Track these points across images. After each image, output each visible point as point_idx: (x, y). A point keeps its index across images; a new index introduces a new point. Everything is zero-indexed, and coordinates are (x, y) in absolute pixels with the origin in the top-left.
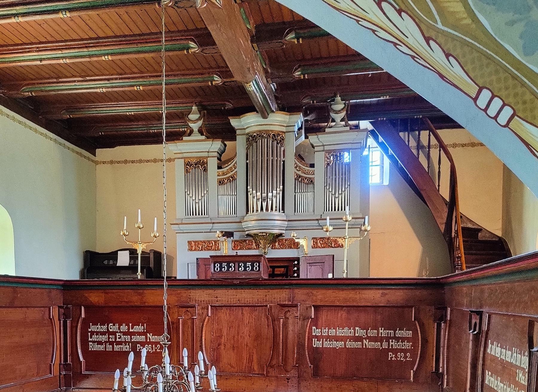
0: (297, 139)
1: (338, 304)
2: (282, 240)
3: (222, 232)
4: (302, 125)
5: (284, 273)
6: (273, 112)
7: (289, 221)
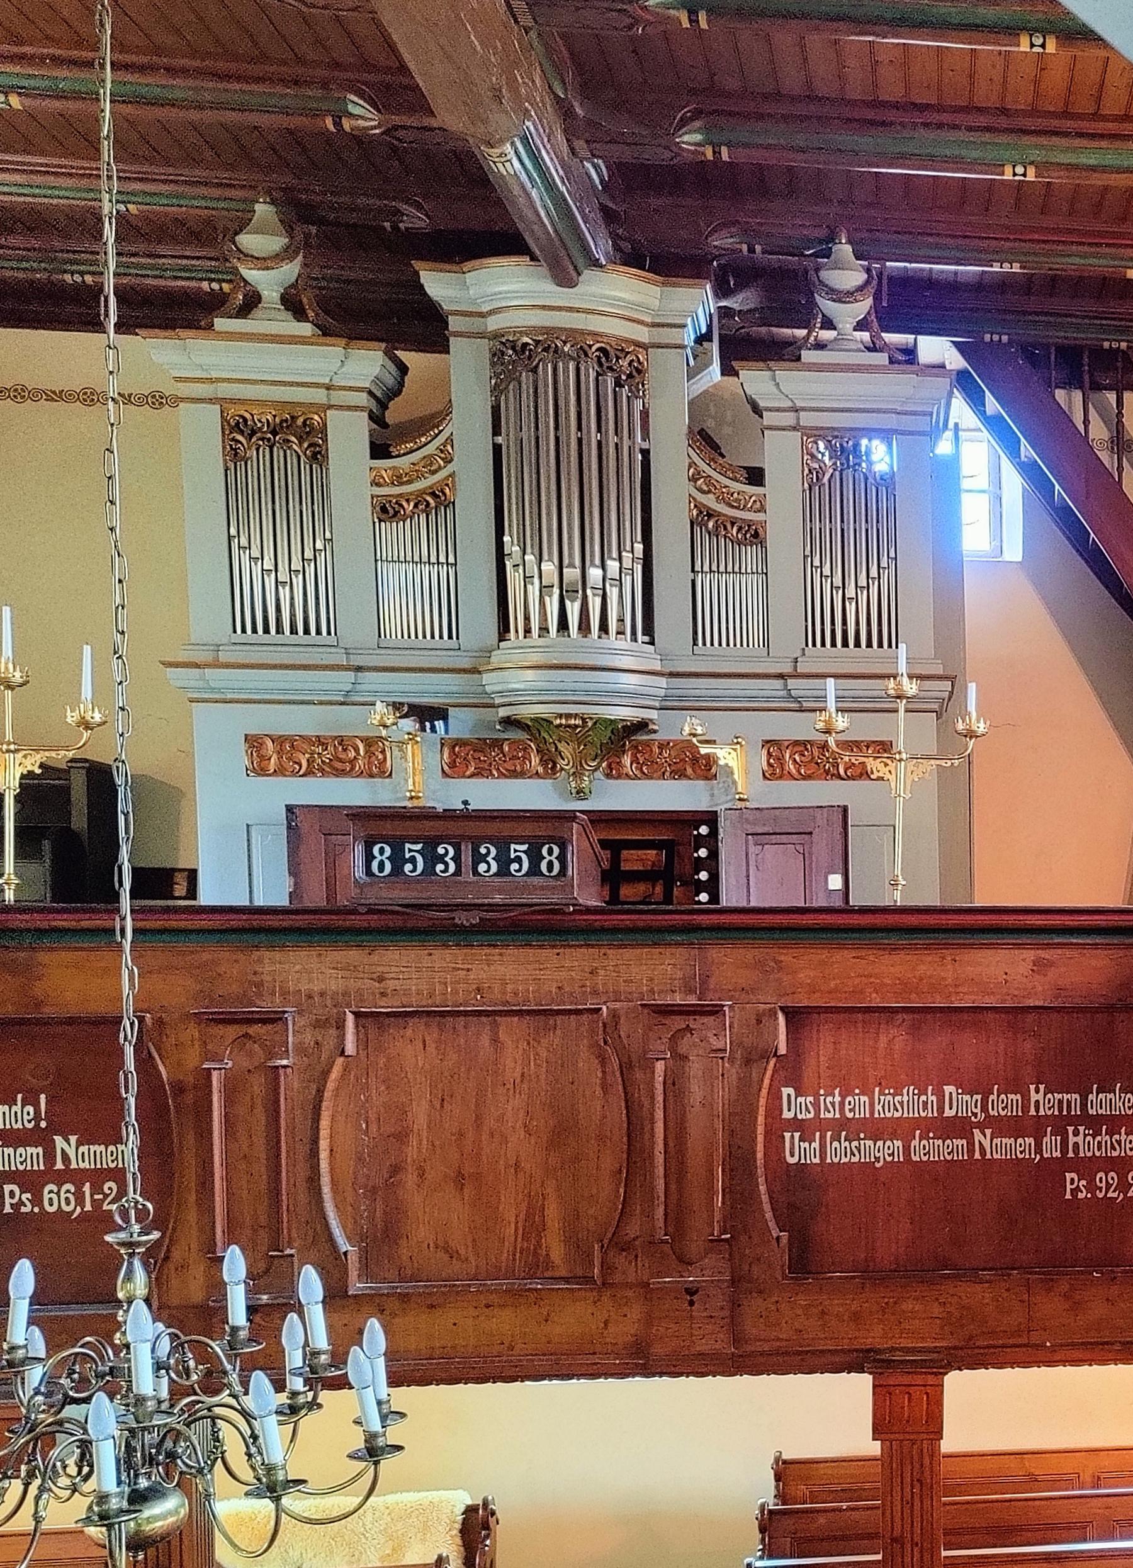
0: (692, 374)
1: (876, 1001)
2: (648, 744)
3: (396, 706)
4: (710, 327)
5: (659, 872)
6: (596, 264)
7: (672, 675)
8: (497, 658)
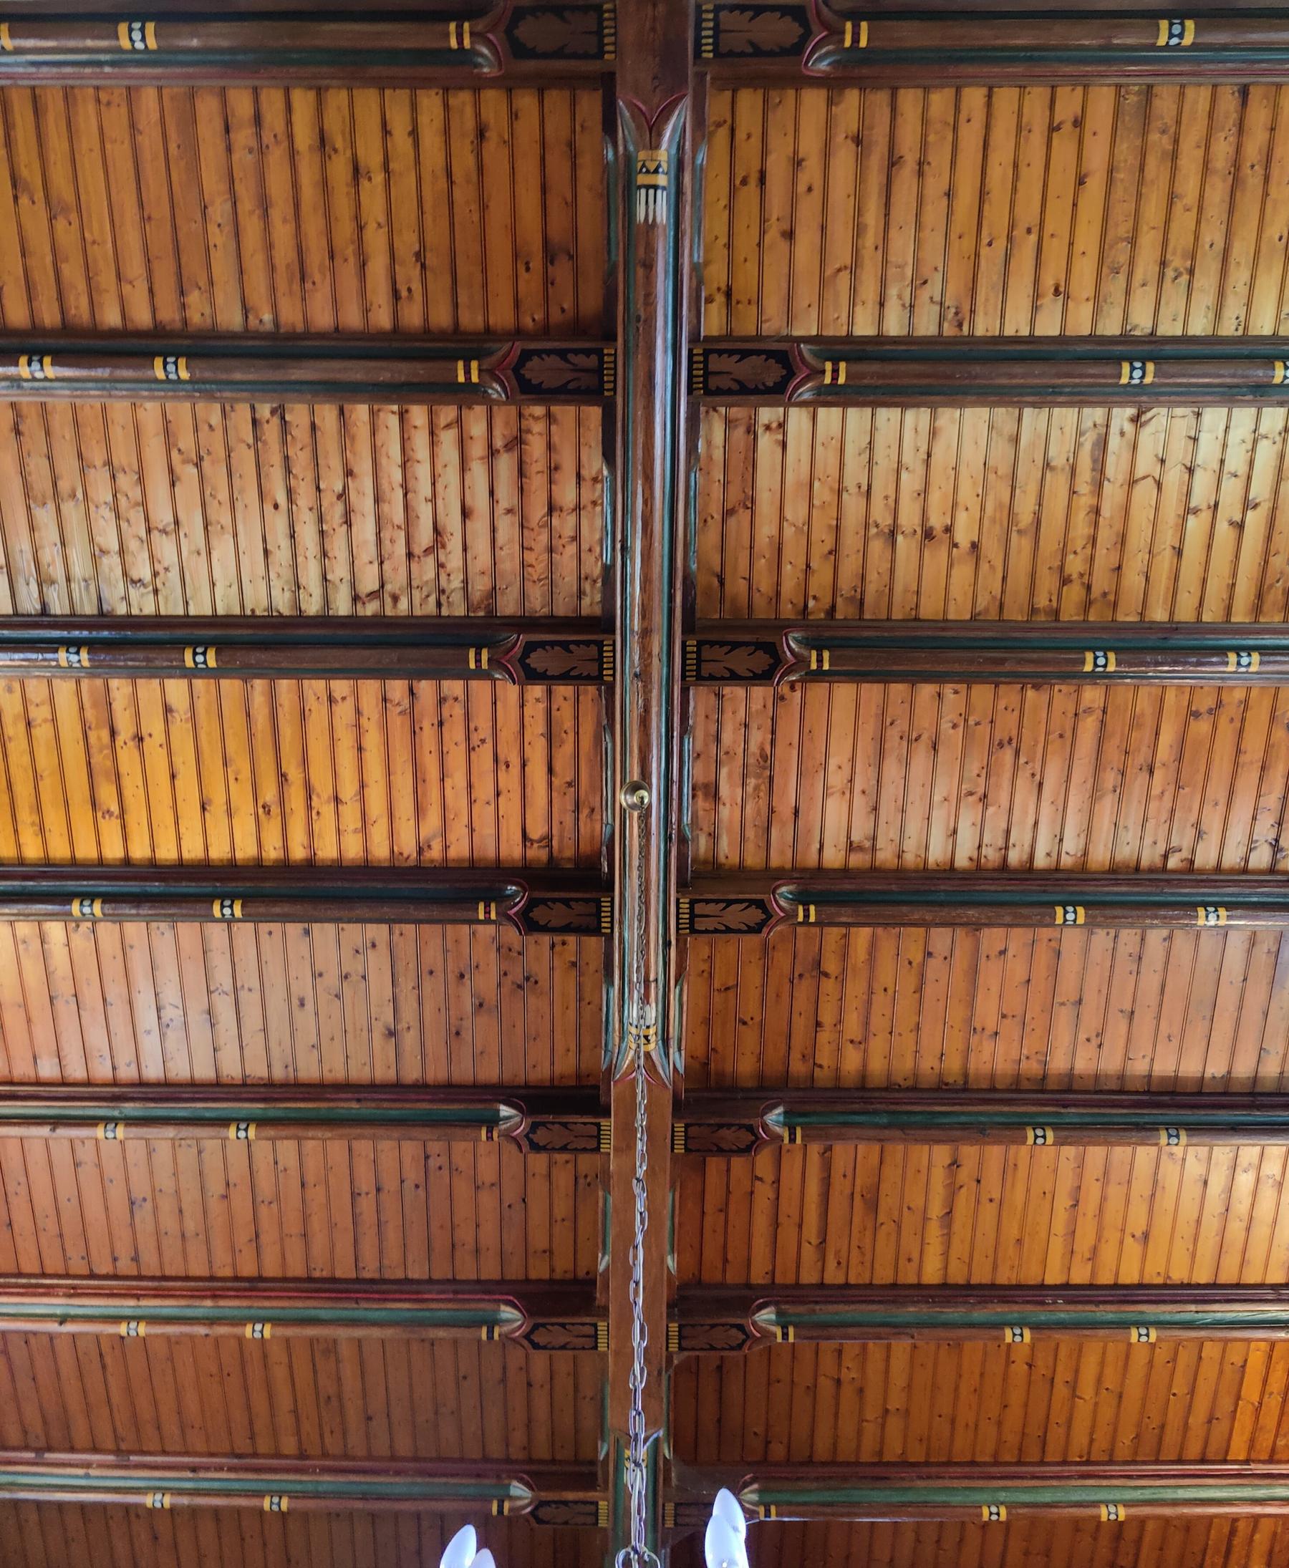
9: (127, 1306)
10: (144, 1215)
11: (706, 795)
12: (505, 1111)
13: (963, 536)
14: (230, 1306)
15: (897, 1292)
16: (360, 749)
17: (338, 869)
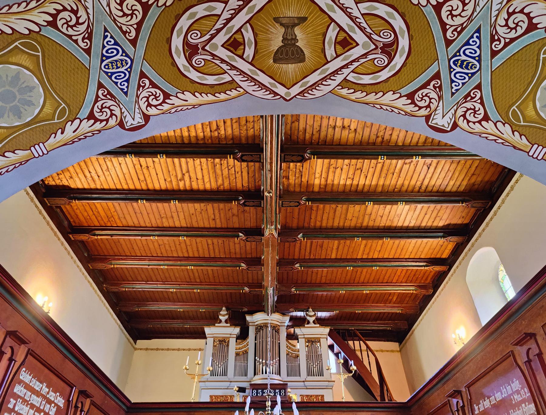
8: (254, 379)
9: (162, 263)
10: (162, 247)
11: (286, 178)
12: (241, 234)
13: (353, 127)
14: (183, 263)
15: (325, 260)
16: (202, 169)
17: (198, 191)
